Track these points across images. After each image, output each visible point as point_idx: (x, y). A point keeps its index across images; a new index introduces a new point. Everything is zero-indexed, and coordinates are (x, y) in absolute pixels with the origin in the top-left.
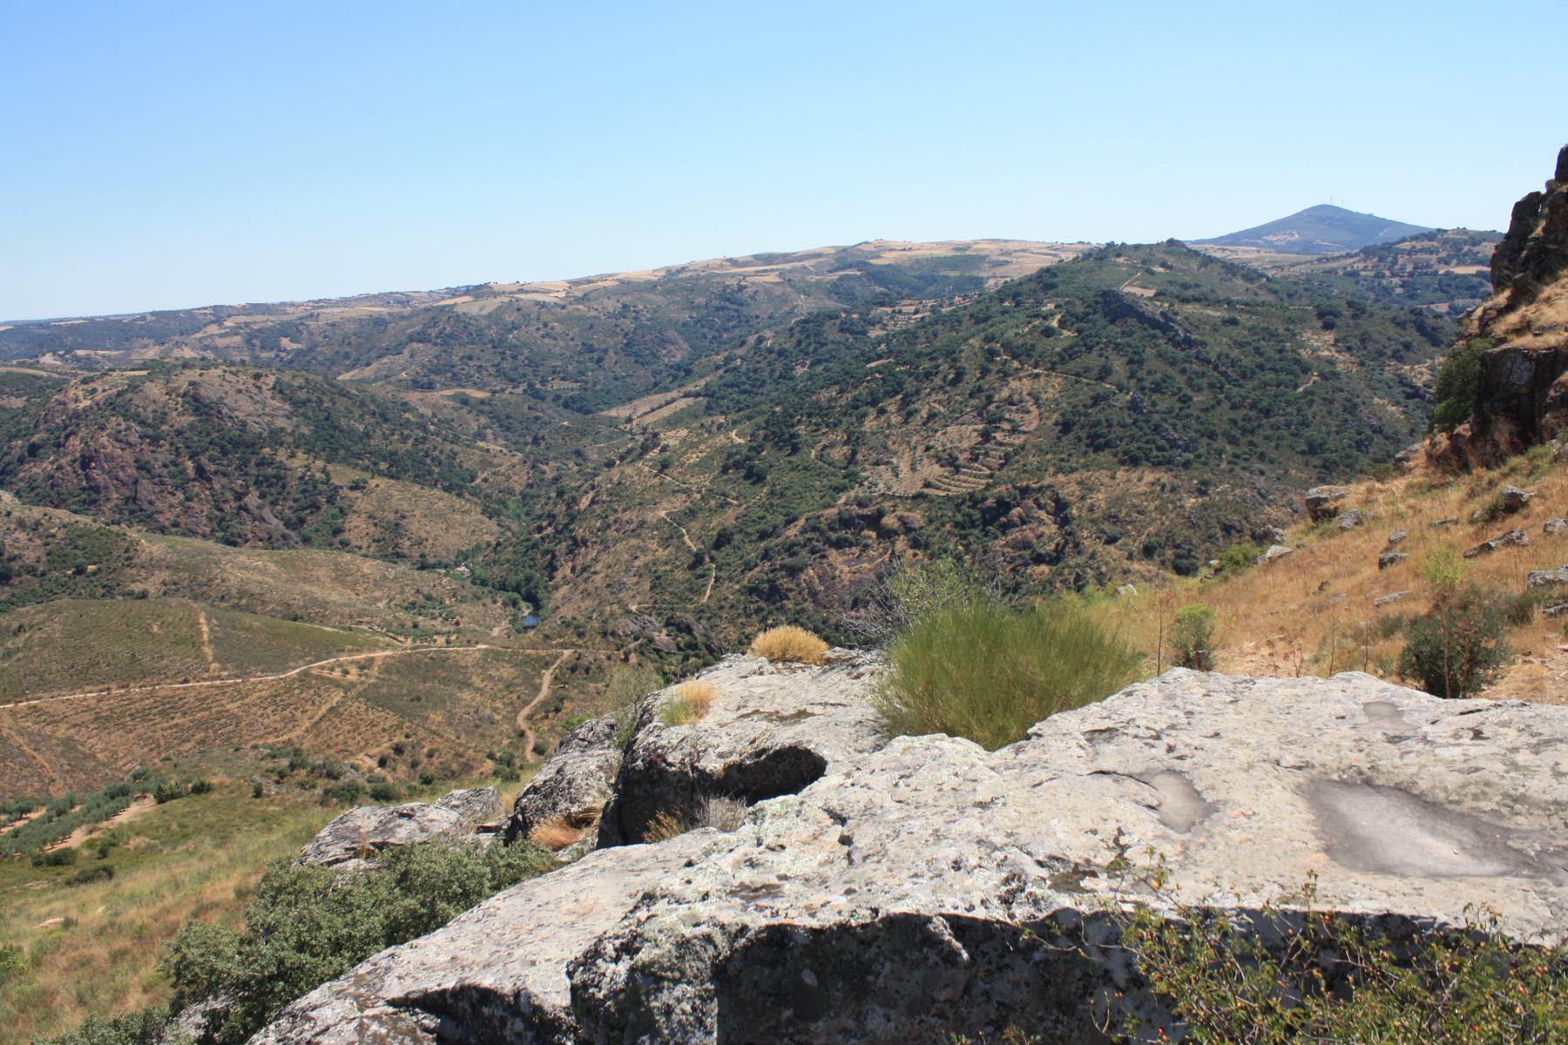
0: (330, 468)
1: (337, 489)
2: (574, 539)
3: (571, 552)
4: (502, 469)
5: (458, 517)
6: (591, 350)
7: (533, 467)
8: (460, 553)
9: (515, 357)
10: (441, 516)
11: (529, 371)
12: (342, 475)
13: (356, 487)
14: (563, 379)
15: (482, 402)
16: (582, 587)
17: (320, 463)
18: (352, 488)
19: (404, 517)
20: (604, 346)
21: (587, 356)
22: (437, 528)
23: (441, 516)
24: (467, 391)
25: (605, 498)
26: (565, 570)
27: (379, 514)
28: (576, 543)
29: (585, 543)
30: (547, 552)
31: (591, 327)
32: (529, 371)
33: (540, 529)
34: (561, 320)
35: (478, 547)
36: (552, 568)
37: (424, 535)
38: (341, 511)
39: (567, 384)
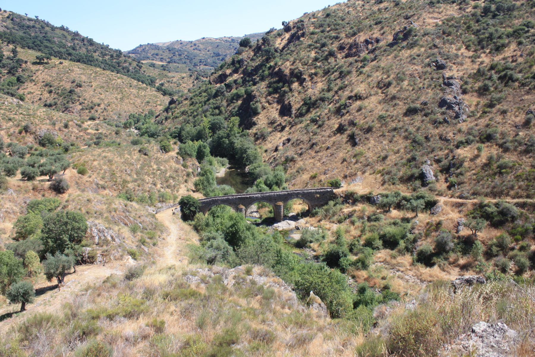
0: (19, 49)
1: (19, 62)
2: (280, 75)
3: (276, 91)
4: (175, 80)
5: (134, 91)
6: (218, 55)
7: (197, 78)
8: (132, 116)
9: (180, 55)
10: (118, 88)
11: (188, 61)
12: (28, 55)
13: (39, 62)
14: (205, 65)
15: (163, 66)
16: (335, 123)
17: (11, 46)
18: (34, 63)
19: (80, 86)
20: (224, 54)
21: (217, 58)
22: (111, 97)
23: (118, 88)
24: (154, 62)
25: (312, 29)
26: (267, 113)
27: (56, 84)
28: (280, 82)
29: (298, 77)
30: (237, 96)
31: (218, 46)
32: (188, 61)
33: (222, 78)
34: (202, 44)
35: (151, 113)
36: (247, 114)
37: (96, 101)
38: (19, 80)
39: (207, 67)
